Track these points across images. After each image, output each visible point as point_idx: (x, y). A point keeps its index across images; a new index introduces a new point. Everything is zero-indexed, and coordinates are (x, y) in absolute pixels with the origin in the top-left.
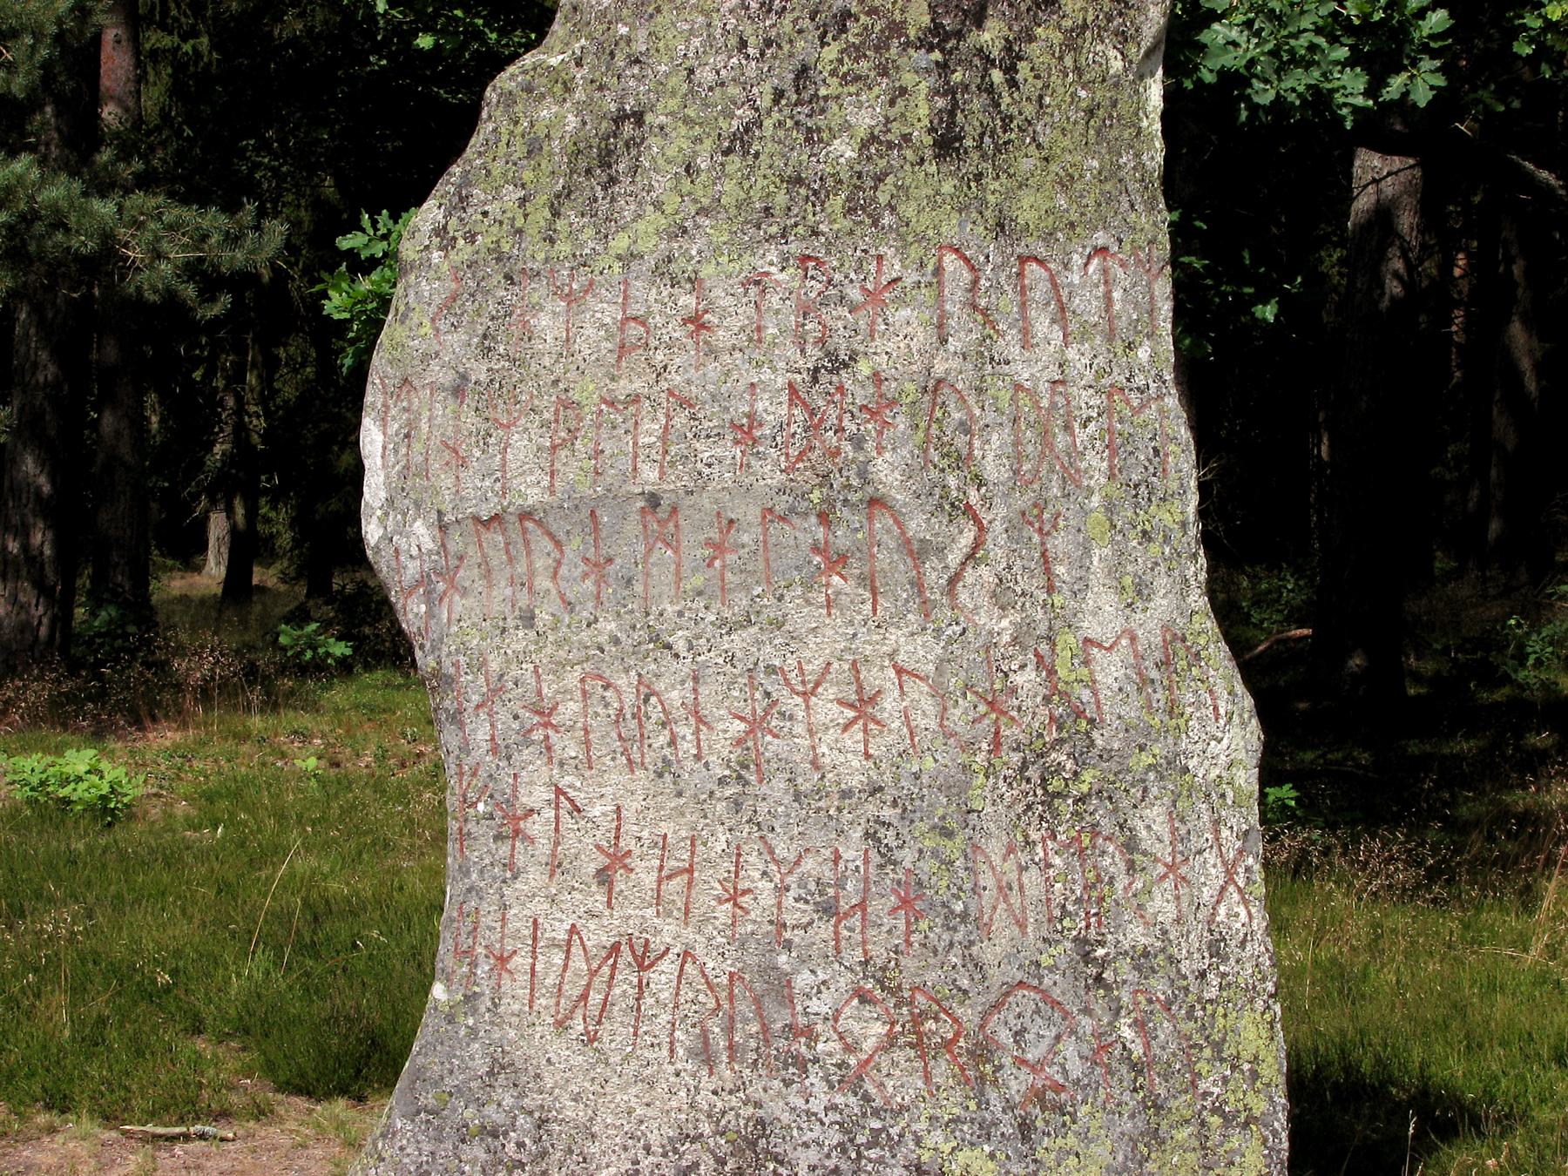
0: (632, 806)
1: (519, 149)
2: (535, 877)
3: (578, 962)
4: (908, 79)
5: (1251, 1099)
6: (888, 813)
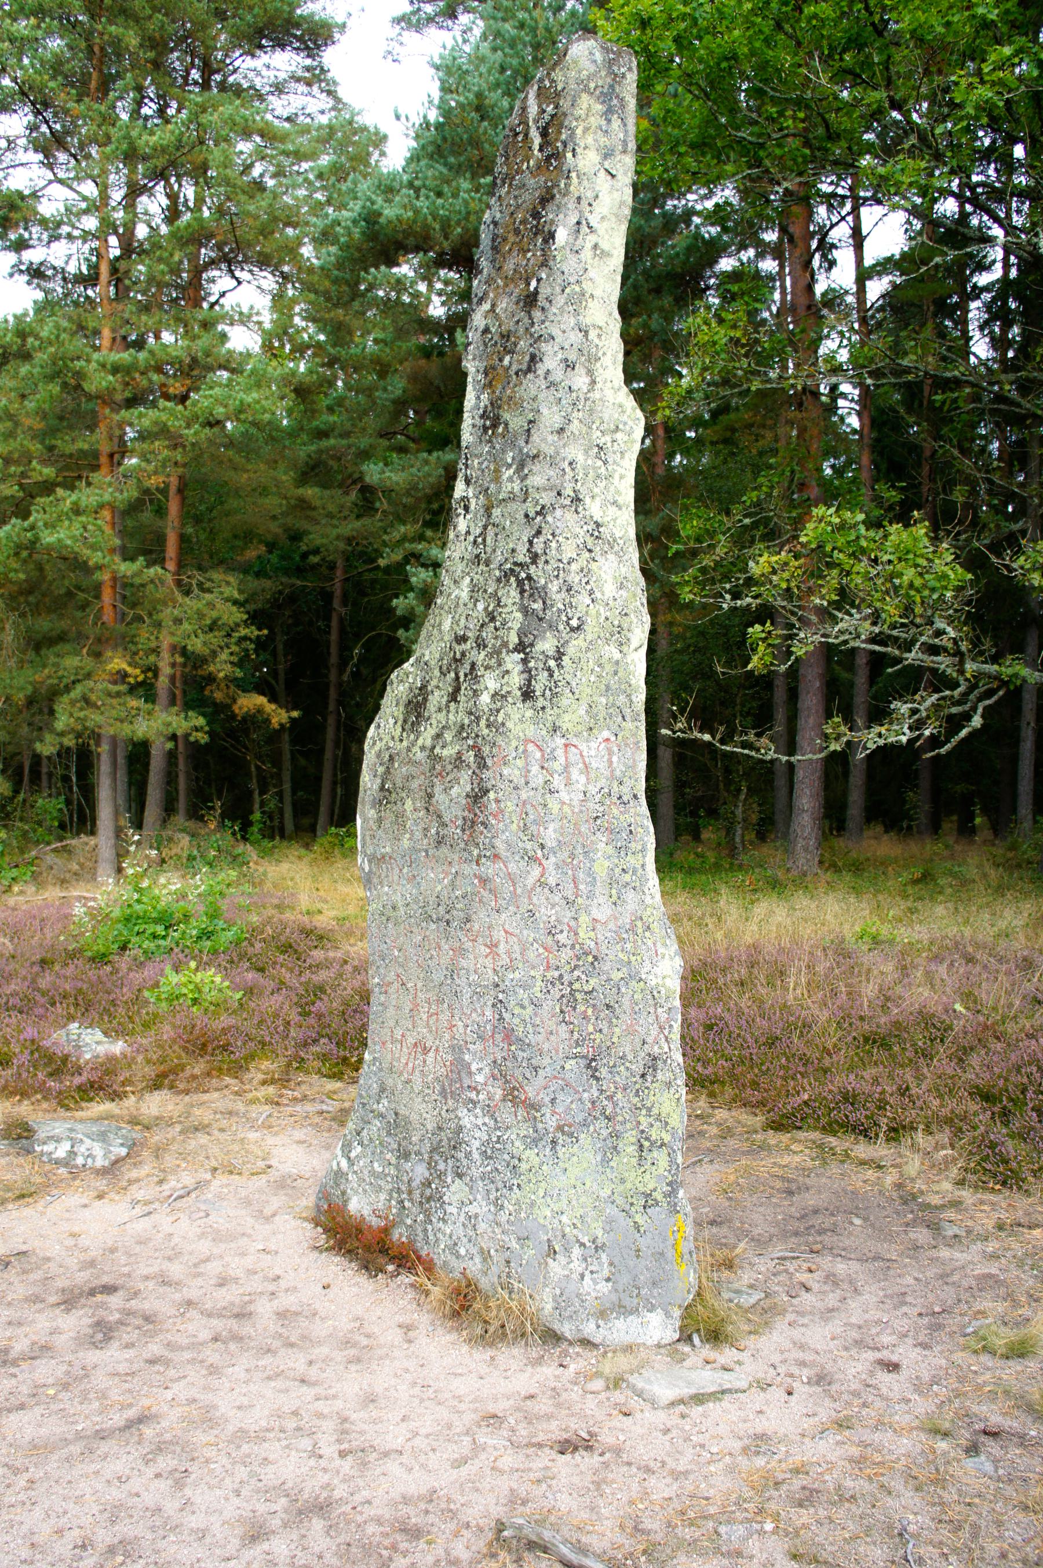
0: (420, 985)
4: (509, 666)
5: (664, 1135)
6: (501, 996)
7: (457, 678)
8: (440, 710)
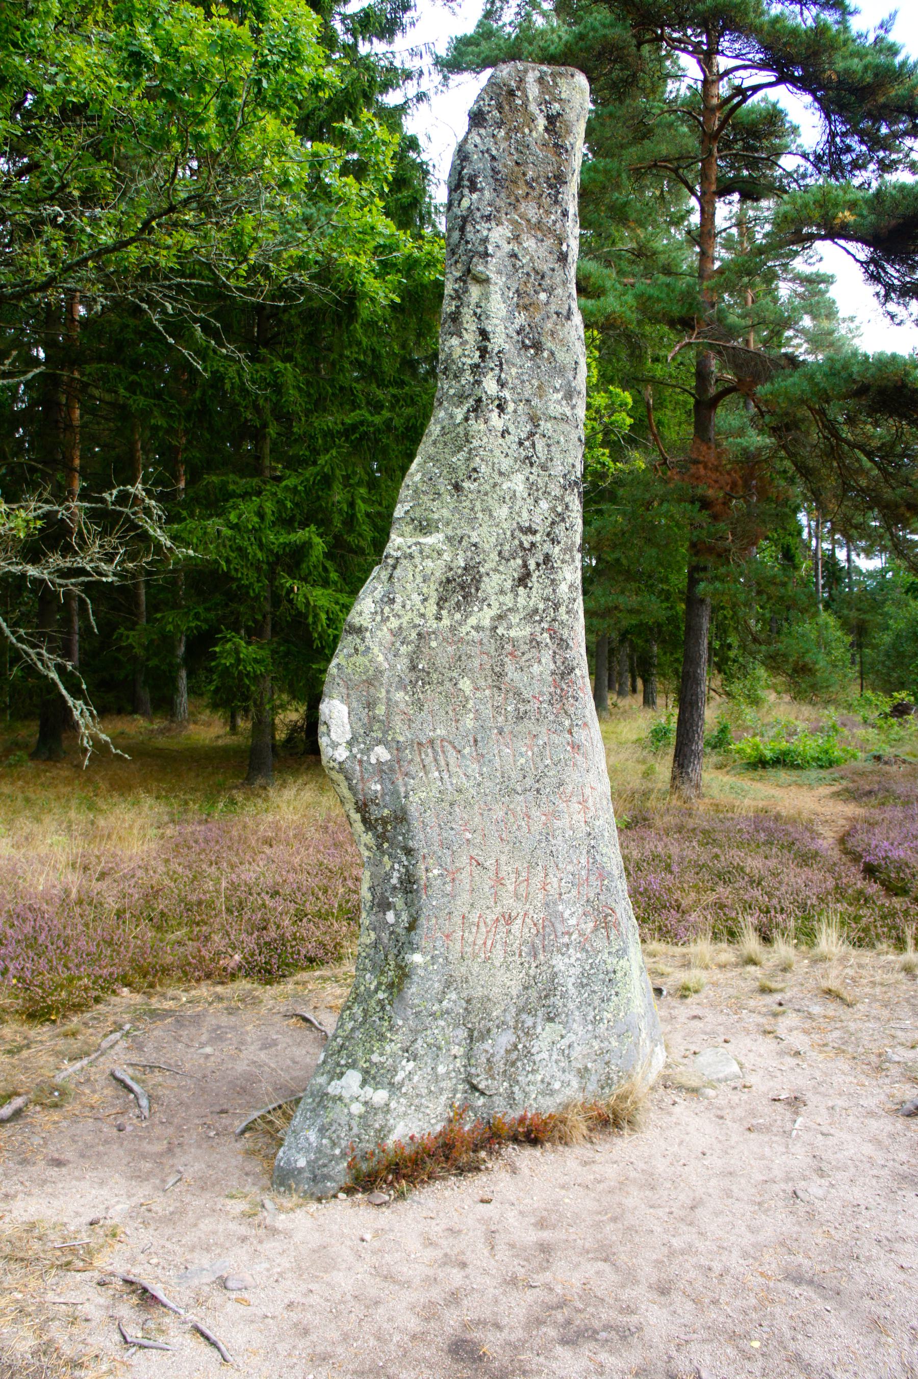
0: (503, 859)
1: (419, 579)
2: (465, 897)
3: (483, 929)
7: (525, 566)
8: (502, 592)
